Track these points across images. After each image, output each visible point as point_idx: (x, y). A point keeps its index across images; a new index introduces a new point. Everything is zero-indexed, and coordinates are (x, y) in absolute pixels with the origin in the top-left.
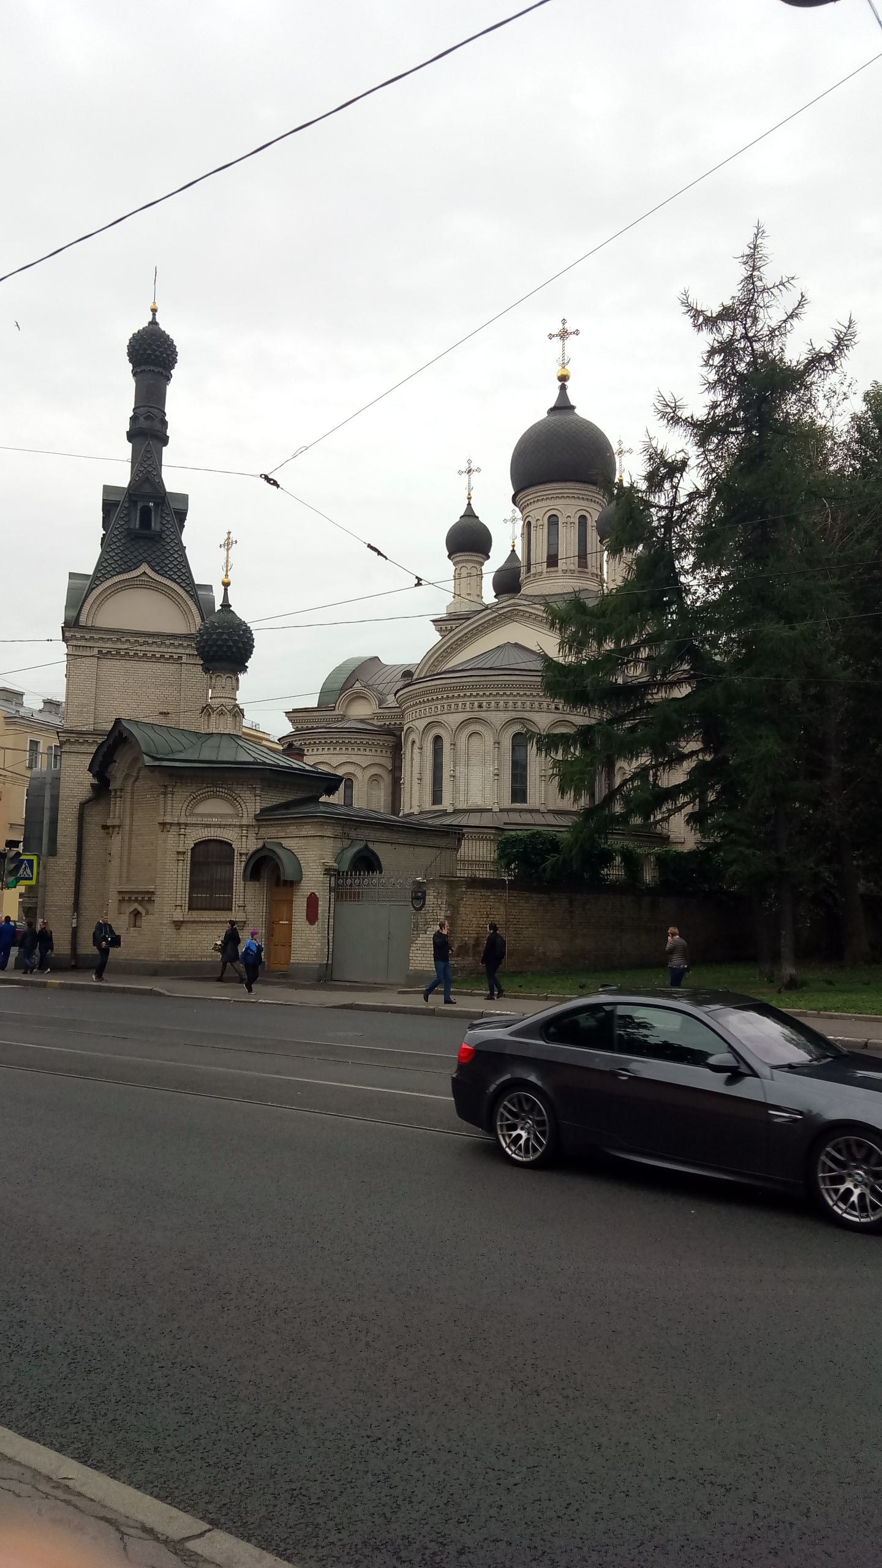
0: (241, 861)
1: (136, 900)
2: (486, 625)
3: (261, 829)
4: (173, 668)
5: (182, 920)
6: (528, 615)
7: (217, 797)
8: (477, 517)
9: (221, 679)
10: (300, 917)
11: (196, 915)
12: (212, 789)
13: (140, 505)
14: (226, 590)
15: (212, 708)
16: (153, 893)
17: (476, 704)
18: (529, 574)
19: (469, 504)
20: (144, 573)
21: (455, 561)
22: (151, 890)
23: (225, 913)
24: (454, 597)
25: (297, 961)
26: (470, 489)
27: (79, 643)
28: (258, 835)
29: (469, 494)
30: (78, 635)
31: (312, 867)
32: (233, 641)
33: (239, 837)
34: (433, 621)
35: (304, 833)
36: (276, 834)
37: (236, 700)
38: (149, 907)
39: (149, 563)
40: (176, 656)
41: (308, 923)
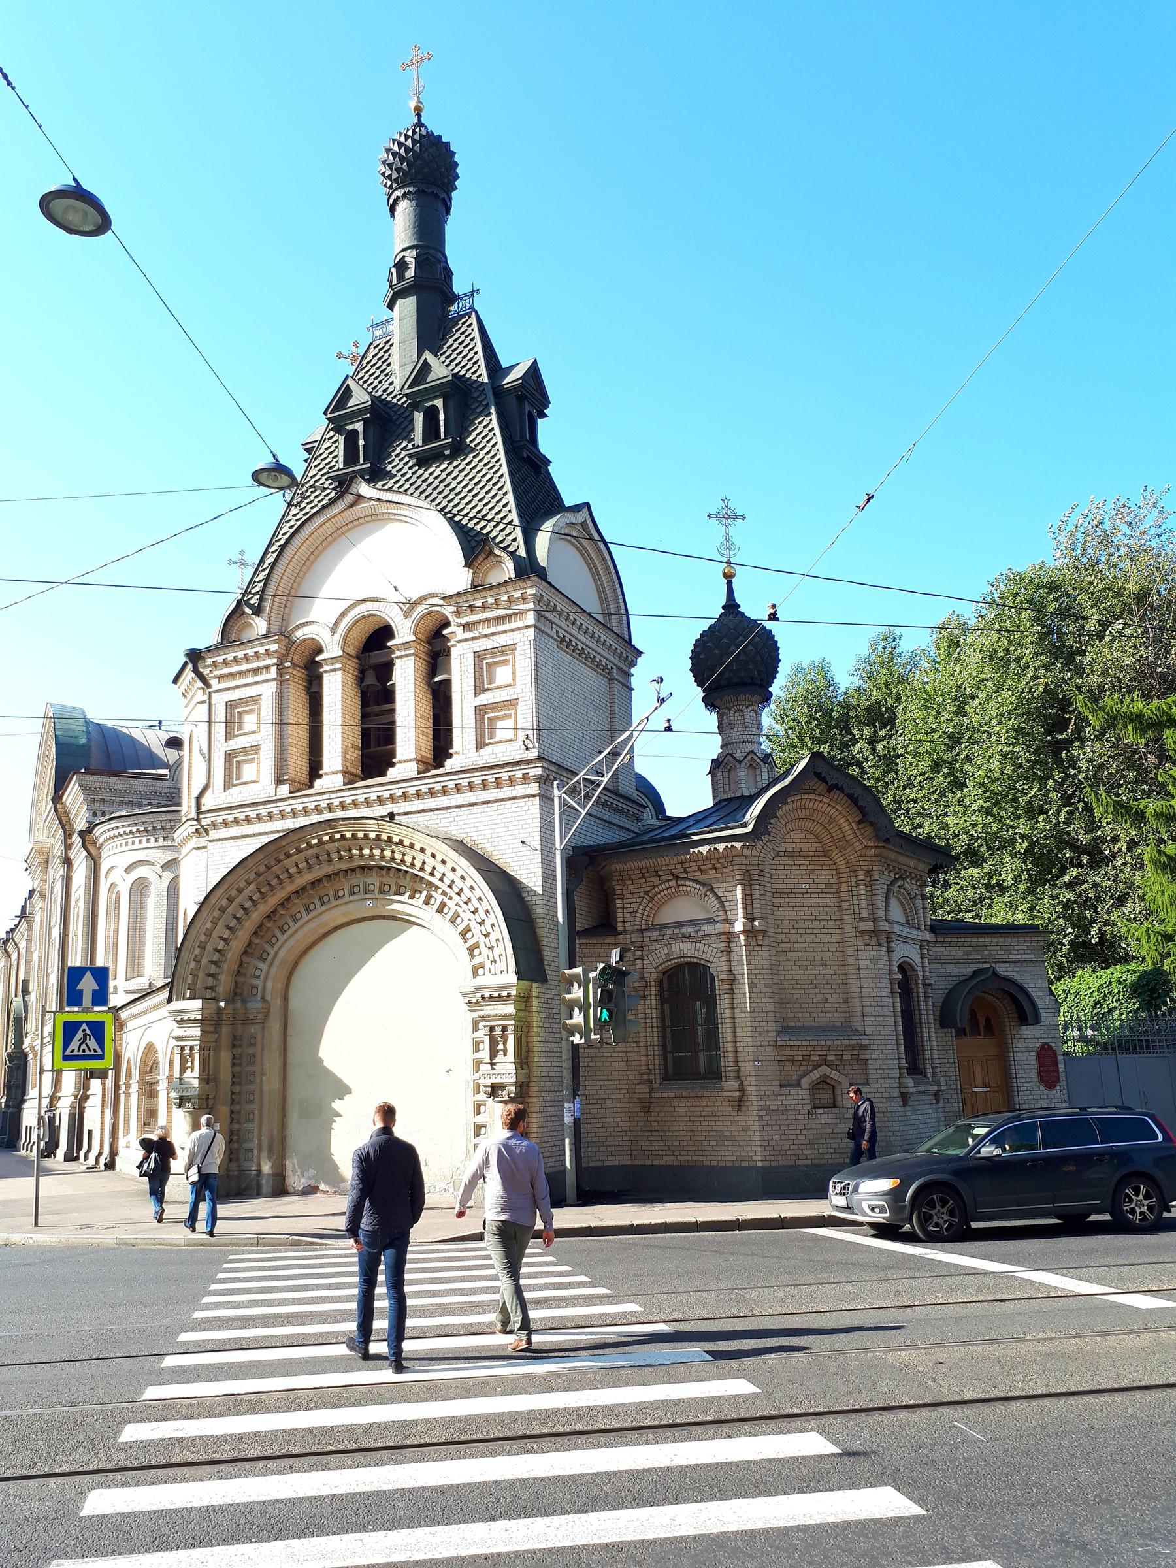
1: (824, 1061)
14: (729, 584)
16: (864, 1047)
41: (1042, 1088)
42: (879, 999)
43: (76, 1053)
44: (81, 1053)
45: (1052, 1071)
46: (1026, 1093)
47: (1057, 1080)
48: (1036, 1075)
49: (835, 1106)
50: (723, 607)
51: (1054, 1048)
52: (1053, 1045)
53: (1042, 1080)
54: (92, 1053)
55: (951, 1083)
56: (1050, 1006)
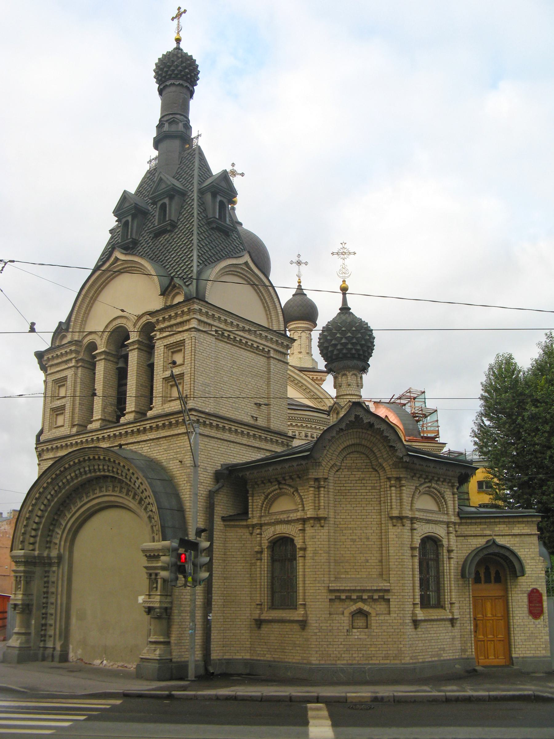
1: (360, 599)
10: (520, 612)
13: (219, 198)
16: (388, 591)
17: (303, 433)
22: (386, 588)
25: (521, 655)
28: (459, 533)
31: (530, 564)
33: (446, 534)
35: (516, 531)
36: (482, 532)
41: (530, 618)
42: (400, 560)
45: (539, 607)
46: (519, 621)
47: (541, 612)
48: (526, 609)
49: (367, 628)
50: (340, 309)
51: (541, 591)
52: (539, 589)
55: (467, 613)
56: (540, 564)
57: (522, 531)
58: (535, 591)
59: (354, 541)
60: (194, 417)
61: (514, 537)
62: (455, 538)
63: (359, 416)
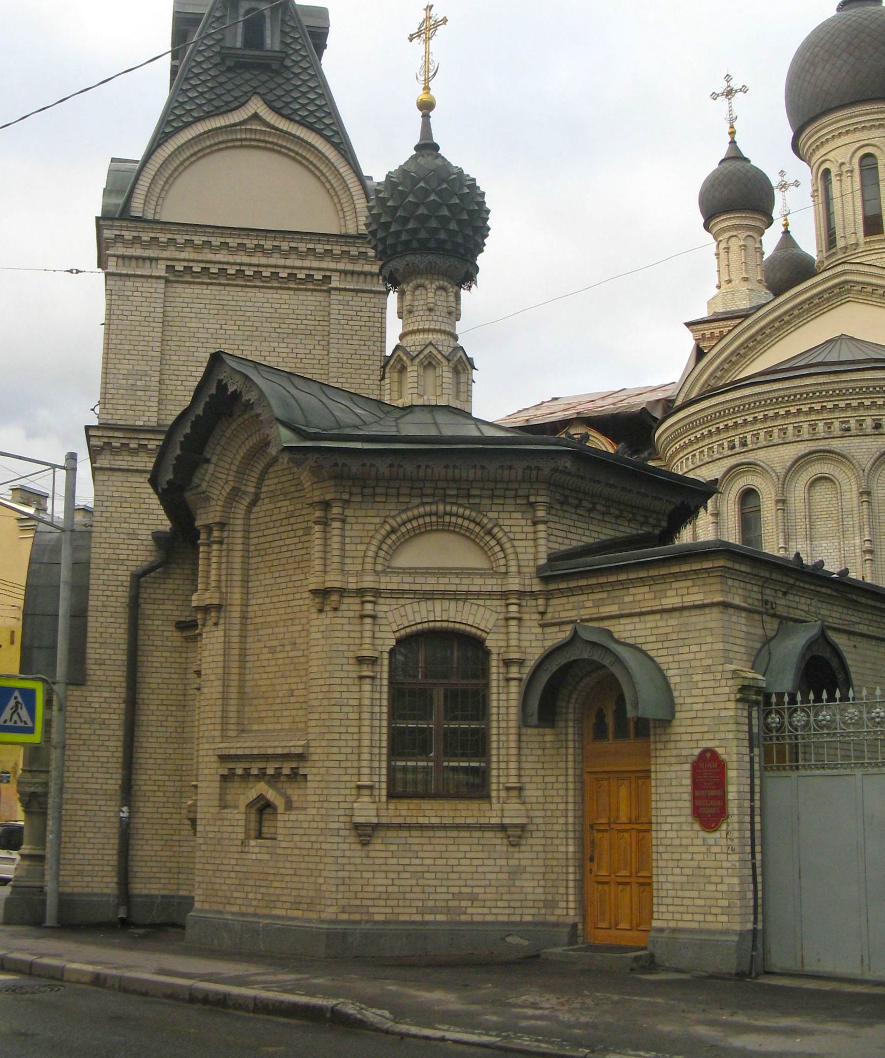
0: (508, 680)
1: (262, 775)
2: (796, 312)
3: (552, 602)
4: (310, 300)
5: (375, 820)
6: (869, 289)
7: (448, 529)
8: (747, 160)
9: (424, 292)
10: (674, 812)
11: (404, 811)
12: (434, 508)
14: (426, 117)
15: (407, 353)
18: (833, 250)
19: (733, 142)
20: (256, 116)
21: (715, 230)
23: (475, 805)
24: (719, 287)
25: (672, 924)
26: (732, 121)
27: (129, 252)
28: (548, 616)
29: (732, 127)
30: (128, 235)
31: (700, 685)
32: (449, 207)
33: (501, 623)
34: (688, 325)
35: (671, 600)
36: (594, 610)
37: (456, 338)
38: (294, 793)
39: (262, 96)
40: (318, 276)
41: (697, 826)
43: (8, 723)
44: (12, 724)
46: (669, 834)
48: (688, 804)
51: (724, 757)
52: (720, 751)
53: (697, 812)
54: (23, 725)
56: (723, 683)
57: (686, 599)
58: (708, 755)
59: (273, 650)
60: (97, 439)
61: (665, 616)
62: (539, 630)
63: (222, 380)
